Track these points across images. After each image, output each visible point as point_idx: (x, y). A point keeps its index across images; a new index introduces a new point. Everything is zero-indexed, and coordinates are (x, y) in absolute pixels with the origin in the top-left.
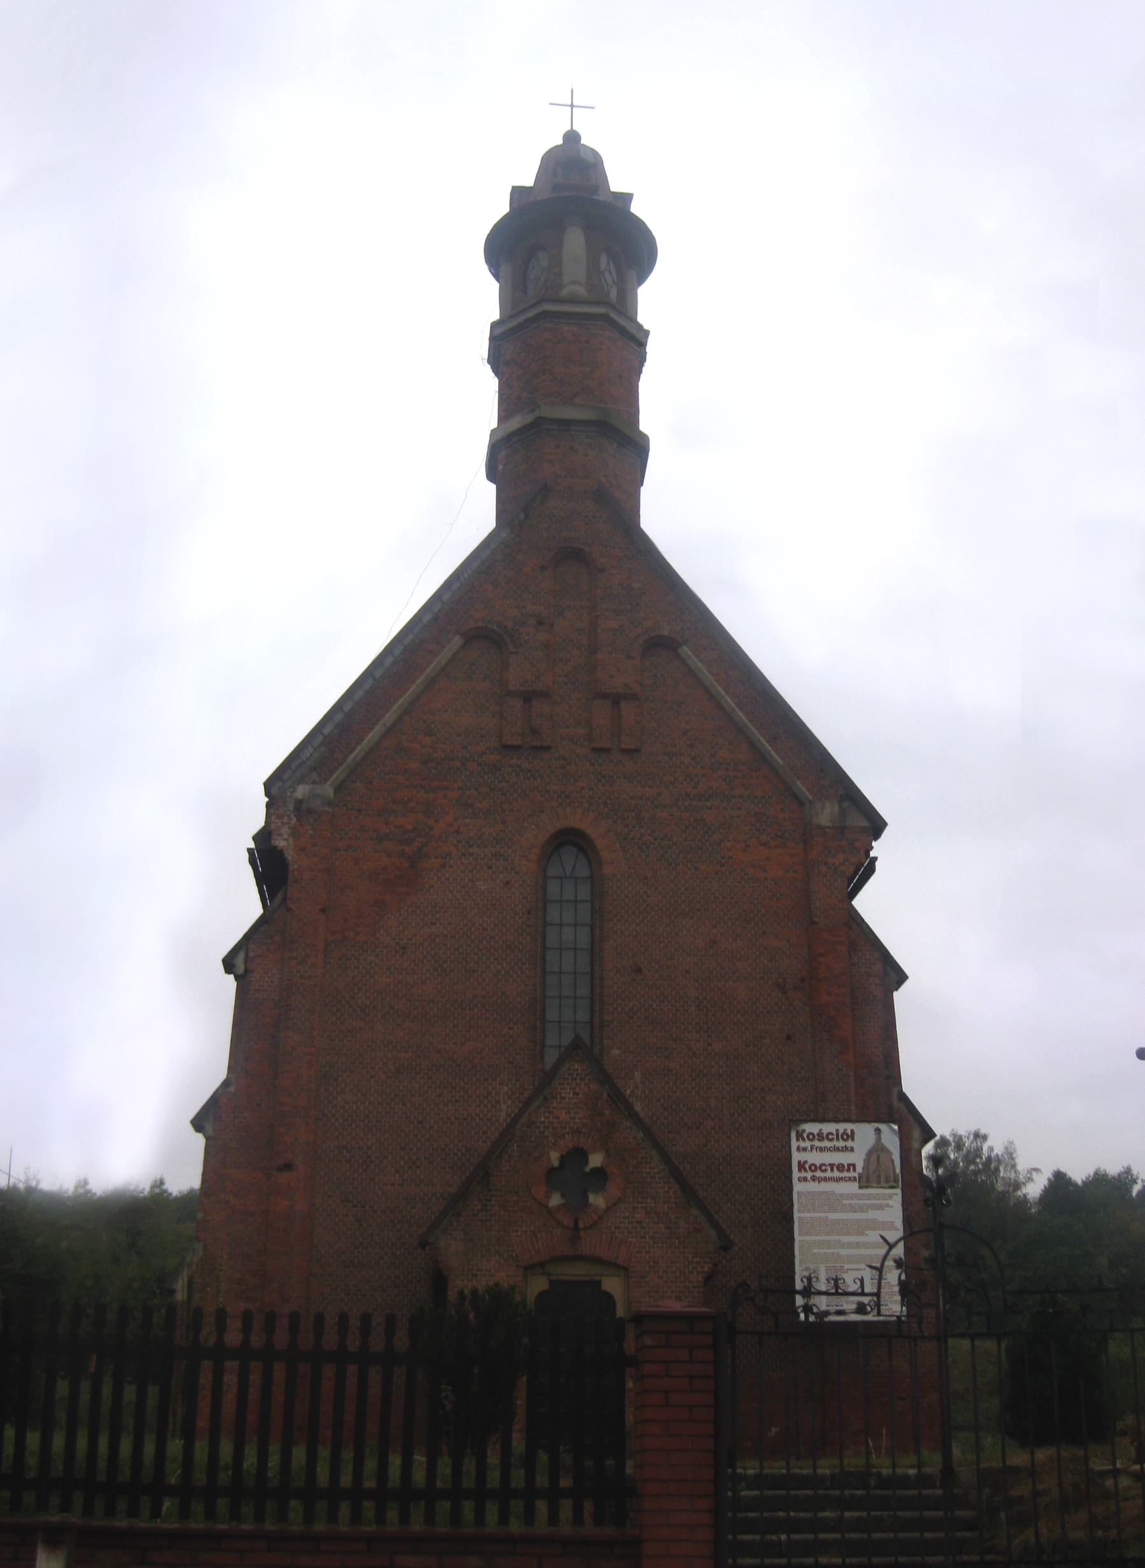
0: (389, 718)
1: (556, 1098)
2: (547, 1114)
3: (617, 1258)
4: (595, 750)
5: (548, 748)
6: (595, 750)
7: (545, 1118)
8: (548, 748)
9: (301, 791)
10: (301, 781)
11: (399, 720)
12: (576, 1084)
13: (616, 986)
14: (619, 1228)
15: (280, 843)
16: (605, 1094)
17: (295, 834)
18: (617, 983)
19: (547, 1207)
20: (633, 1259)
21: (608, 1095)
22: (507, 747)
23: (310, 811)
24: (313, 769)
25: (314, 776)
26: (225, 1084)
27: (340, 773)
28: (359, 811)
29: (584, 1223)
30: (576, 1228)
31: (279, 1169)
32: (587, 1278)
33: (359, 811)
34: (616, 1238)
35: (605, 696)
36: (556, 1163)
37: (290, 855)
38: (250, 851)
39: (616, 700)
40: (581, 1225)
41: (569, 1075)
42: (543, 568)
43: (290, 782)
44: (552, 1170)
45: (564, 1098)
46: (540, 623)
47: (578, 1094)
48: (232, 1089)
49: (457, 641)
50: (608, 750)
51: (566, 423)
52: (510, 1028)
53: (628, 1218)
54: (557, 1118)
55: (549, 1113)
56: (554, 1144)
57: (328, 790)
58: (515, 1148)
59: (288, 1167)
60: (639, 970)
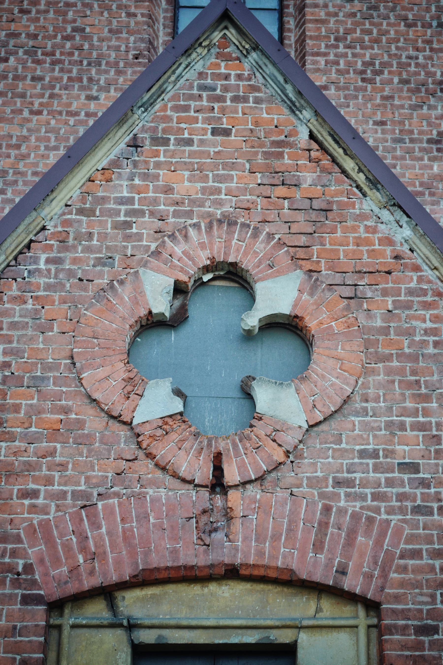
1: (166, 142)
2: (137, 181)
3: (342, 571)
7: (132, 188)
12: (223, 110)
13: (332, 20)
14: (349, 483)
16: (304, 135)
18: (336, 15)
19: (129, 424)
20: (393, 575)
21: (312, 136)
29: (242, 467)
34: (342, 511)
41: (203, 88)
45: (190, 142)
47: (227, 132)
52: (89, 98)
53: (375, 454)
54: (168, 190)
55: (145, 177)
56: (157, 253)
58: (42, 266)
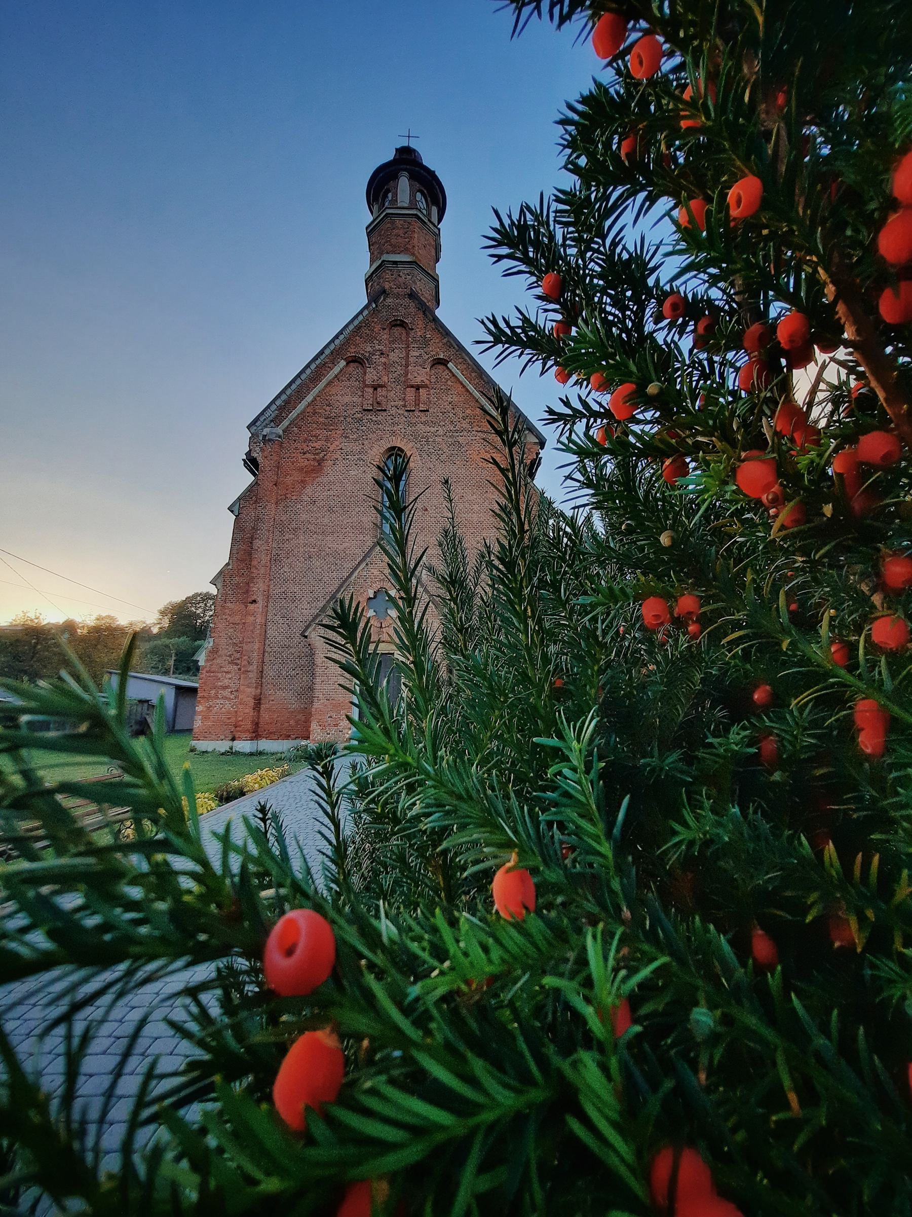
0: (309, 398)
4: (406, 411)
5: (385, 410)
6: (406, 411)
8: (385, 410)
9: (266, 431)
10: (266, 426)
11: (315, 399)
15: (255, 455)
17: (262, 450)
22: (365, 410)
23: (270, 440)
24: (272, 421)
25: (272, 424)
26: (227, 564)
27: (286, 423)
28: (295, 441)
30: (381, 627)
31: (252, 603)
32: (387, 652)
33: (295, 441)
35: (412, 386)
36: (372, 596)
37: (260, 460)
38: (244, 460)
39: (418, 388)
40: (383, 626)
42: (384, 329)
43: (260, 428)
44: (370, 598)
46: (382, 354)
48: (230, 567)
49: (343, 363)
50: (414, 411)
51: (395, 263)
57: (279, 431)
59: (254, 601)
60: (426, 510)
